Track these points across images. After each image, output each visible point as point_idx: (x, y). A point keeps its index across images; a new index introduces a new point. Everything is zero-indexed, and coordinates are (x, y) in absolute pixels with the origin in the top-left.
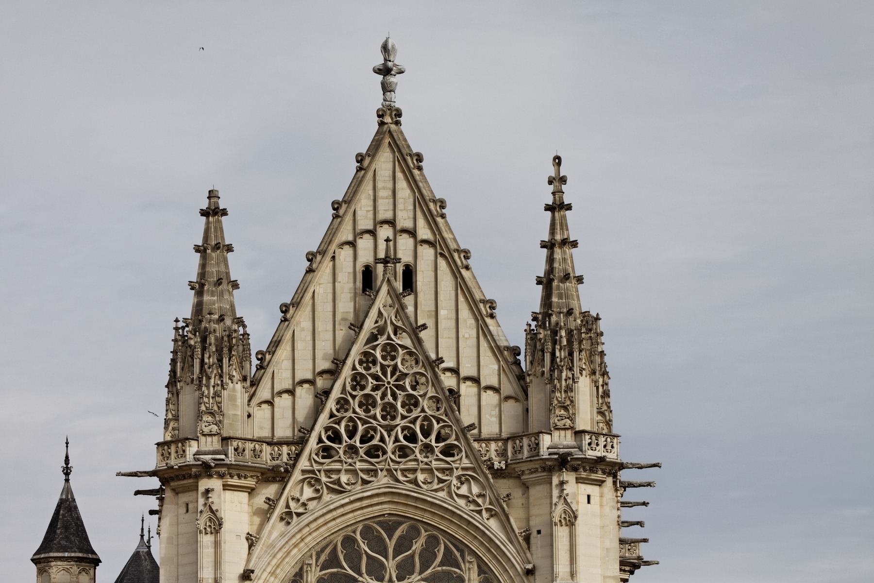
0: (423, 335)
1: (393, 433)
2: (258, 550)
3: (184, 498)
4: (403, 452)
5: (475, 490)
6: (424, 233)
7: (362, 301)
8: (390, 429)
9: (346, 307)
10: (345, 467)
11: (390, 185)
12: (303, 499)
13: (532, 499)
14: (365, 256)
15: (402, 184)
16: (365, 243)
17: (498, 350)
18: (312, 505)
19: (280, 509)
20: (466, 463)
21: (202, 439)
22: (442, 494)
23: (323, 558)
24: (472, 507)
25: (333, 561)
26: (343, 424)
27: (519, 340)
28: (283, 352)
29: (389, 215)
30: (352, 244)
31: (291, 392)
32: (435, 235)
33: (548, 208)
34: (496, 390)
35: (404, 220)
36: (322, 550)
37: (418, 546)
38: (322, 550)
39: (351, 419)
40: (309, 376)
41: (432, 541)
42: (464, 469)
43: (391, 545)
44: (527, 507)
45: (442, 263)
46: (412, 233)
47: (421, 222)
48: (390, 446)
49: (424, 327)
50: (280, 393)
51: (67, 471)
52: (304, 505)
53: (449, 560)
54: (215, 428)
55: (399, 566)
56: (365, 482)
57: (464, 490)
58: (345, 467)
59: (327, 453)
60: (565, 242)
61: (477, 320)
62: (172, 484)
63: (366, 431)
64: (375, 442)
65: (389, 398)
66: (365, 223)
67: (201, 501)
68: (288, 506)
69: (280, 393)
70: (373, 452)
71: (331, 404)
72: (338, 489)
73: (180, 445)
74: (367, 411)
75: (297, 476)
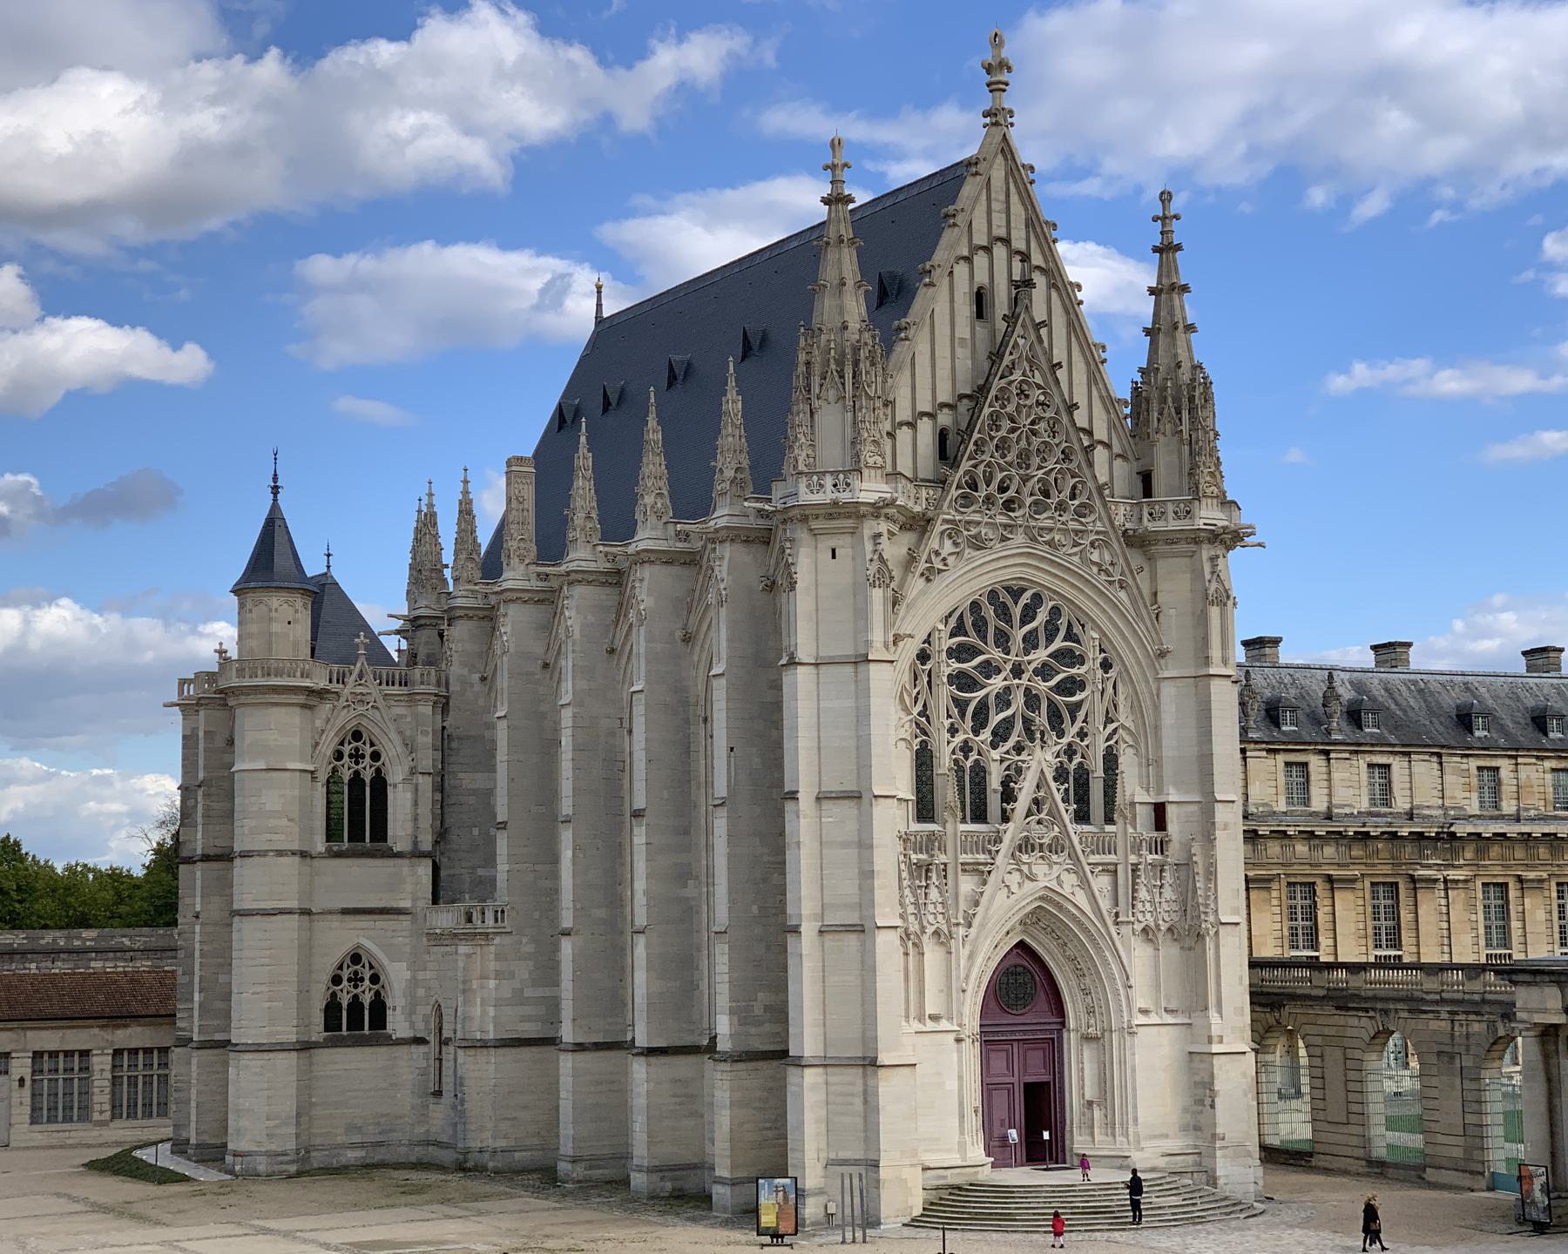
0: (1059, 373)
1: (1029, 484)
2: (902, 609)
3: (826, 544)
4: (1039, 507)
5: (1107, 558)
6: (1037, 259)
7: (981, 331)
8: (1025, 480)
9: (963, 331)
10: (986, 519)
11: (1002, 197)
12: (944, 554)
13: (1160, 573)
14: (982, 278)
15: (1014, 198)
16: (981, 260)
17: (1110, 402)
18: (951, 560)
19: (922, 566)
20: (1099, 527)
21: (866, 472)
22: (1076, 559)
23: (953, 622)
24: (1103, 577)
25: (959, 630)
26: (982, 467)
27: (1123, 392)
28: (904, 379)
29: (1002, 232)
30: (968, 260)
31: (912, 425)
32: (1046, 261)
33: (1156, 250)
34: (1108, 446)
35: (1019, 243)
36: (950, 615)
37: (1042, 616)
38: (950, 615)
39: (989, 465)
40: (928, 409)
41: (1055, 612)
42: (1098, 533)
43: (1017, 612)
44: (1153, 578)
45: (1054, 295)
46: (1025, 257)
47: (1033, 245)
48: (1029, 501)
49: (1059, 365)
50: (901, 424)
51: (275, 490)
52: (944, 559)
53: (1070, 636)
54: (879, 460)
55: (1024, 639)
56: (1004, 539)
57: (1095, 557)
58: (986, 519)
59: (966, 500)
60: (1173, 287)
61: (1088, 364)
62: (814, 525)
63: (1002, 481)
64: (1011, 493)
65: (1023, 443)
66: (981, 239)
67: (869, 547)
68: (929, 561)
69: (901, 424)
70: (1009, 505)
71: (971, 447)
72: (978, 544)
73: (841, 476)
74: (1003, 456)
75: (939, 527)
